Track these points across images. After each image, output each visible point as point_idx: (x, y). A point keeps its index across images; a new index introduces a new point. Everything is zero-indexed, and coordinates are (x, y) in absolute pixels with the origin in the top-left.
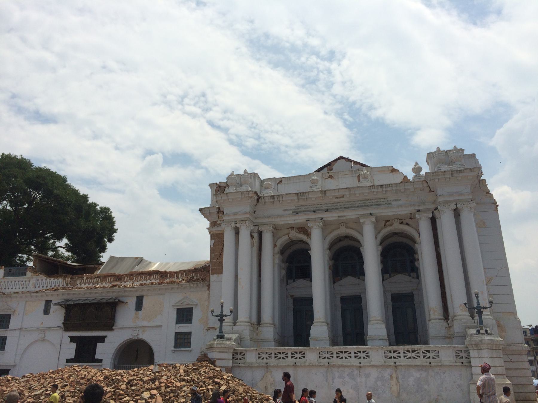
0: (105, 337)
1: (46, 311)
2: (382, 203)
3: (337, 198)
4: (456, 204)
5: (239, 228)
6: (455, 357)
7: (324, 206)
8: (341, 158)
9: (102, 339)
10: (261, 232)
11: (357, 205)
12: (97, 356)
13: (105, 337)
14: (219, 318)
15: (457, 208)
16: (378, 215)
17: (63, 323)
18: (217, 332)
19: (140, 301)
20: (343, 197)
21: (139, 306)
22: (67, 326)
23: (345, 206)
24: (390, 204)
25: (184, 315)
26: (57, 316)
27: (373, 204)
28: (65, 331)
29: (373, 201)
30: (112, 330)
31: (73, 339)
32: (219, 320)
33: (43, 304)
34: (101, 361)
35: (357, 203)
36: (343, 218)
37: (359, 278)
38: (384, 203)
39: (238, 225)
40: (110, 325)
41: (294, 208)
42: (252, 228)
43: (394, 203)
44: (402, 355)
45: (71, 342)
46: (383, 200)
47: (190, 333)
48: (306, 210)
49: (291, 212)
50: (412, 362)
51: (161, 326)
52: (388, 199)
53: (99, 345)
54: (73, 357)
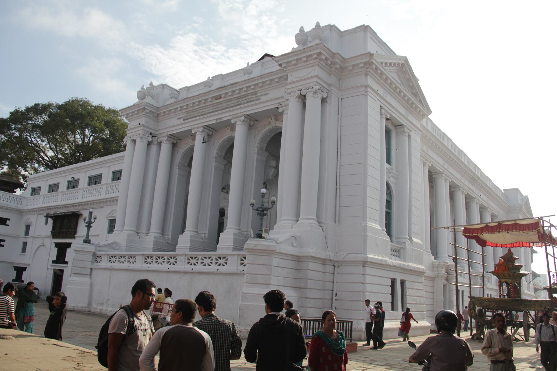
1: (46, 223)
2: (252, 99)
3: (216, 100)
6: (239, 264)
8: (266, 55)
9: (69, 245)
10: (161, 142)
16: (248, 113)
17: (52, 232)
18: (84, 238)
20: (220, 98)
22: (55, 234)
24: (260, 99)
27: (246, 101)
29: (246, 98)
30: (74, 238)
31: (57, 245)
32: (86, 226)
34: (67, 263)
35: (232, 102)
39: (134, 138)
41: (185, 115)
42: (150, 139)
43: (262, 98)
44: (200, 261)
46: (254, 96)
48: (193, 116)
49: (182, 119)
50: (207, 269)
51: (98, 235)
52: (259, 94)
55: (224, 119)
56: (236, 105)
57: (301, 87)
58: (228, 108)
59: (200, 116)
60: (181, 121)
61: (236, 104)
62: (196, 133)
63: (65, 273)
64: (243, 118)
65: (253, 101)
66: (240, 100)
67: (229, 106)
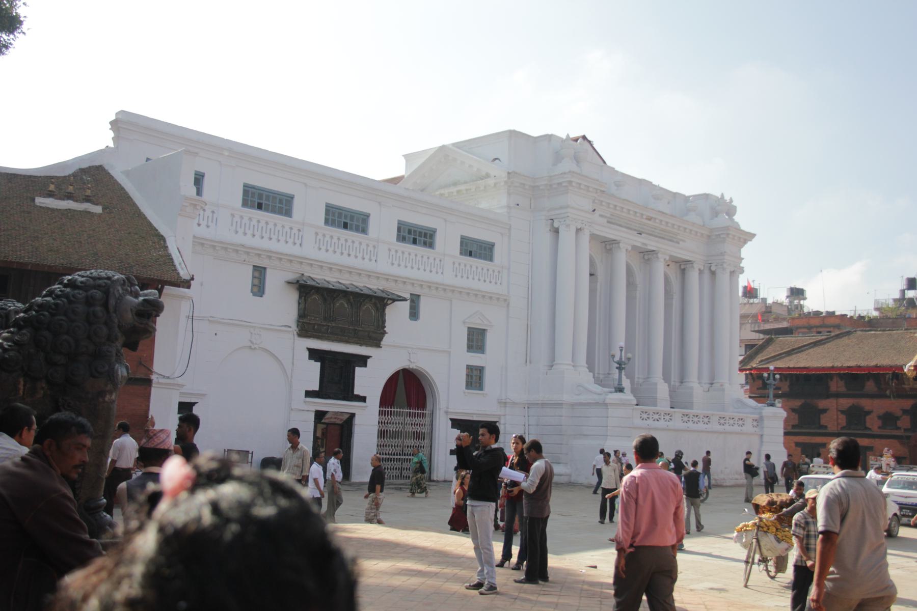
0: (369, 357)
9: (363, 361)
12: (356, 393)
13: (369, 357)
19: (415, 300)
21: (414, 314)
22: (305, 329)
25: (476, 339)
26: (283, 307)
28: (300, 335)
30: (378, 345)
31: (314, 354)
33: (249, 272)
34: (363, 399)
40: (375, 337)
45: (310, 358)
47: (481, 370)
53: (358, 370)
54: (317, 388)
63: (357, 420)
64: (668, 258)
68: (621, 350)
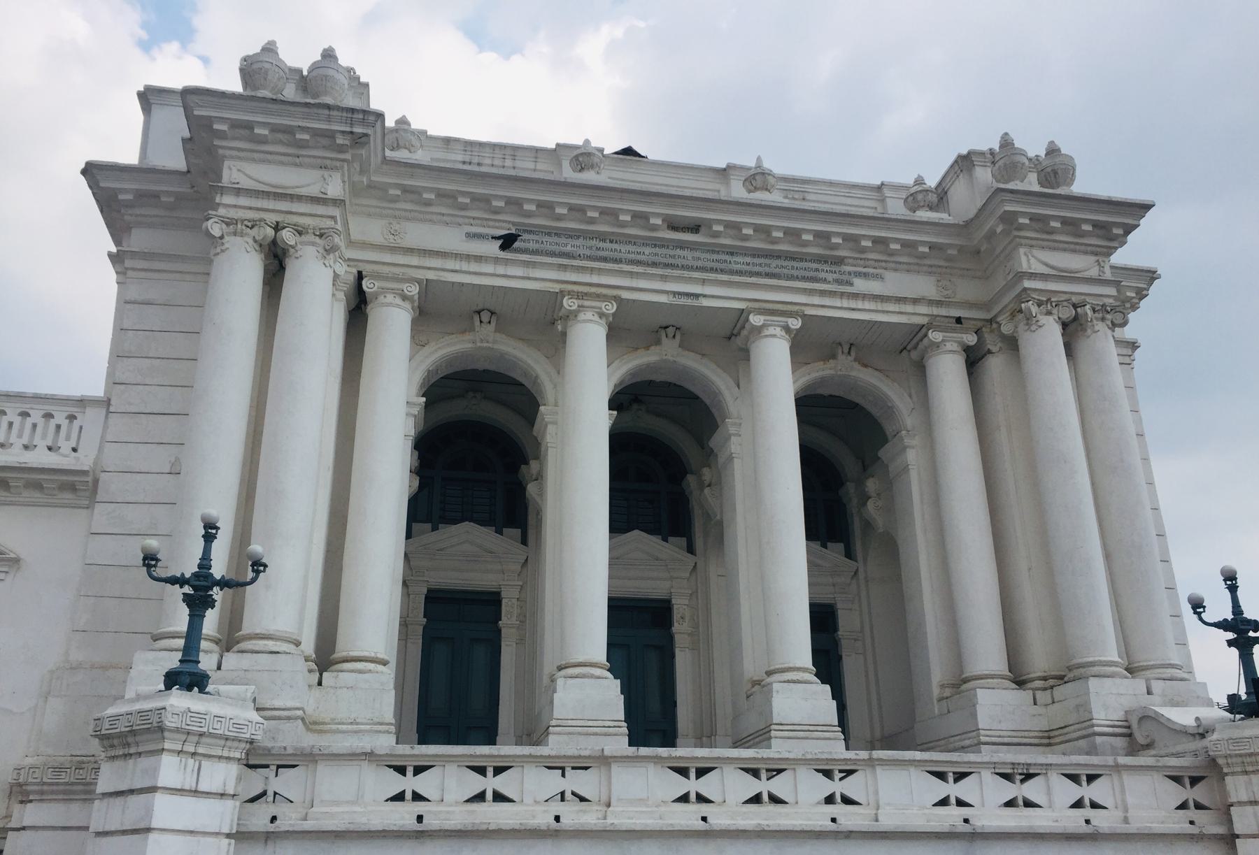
2: (822, 275)
4: (1075, 306)
5: (285, 252)
7: (624, 248)
11: (739, 267)
14: (187, 589)
15: (1076, 318)
20: (695, 228)
23: (700, 264)
27: (795, 273)
29: (795, 264)
35: (740, 259)
36: (689, 302)
37: (665, 540)
38: (830, 277)
46: (826, 267)
55: (706, 303)
56: (758, 274)
57: (1074, 299)
58: (722, 271)
59: (590, 258)
60: (493, 248)
61: (757, 269)
62: (575, 314)
64: (796, 324)
65: (825, 281)
66: (775, 263)
67: (723, 266)
68: (209, 538)
